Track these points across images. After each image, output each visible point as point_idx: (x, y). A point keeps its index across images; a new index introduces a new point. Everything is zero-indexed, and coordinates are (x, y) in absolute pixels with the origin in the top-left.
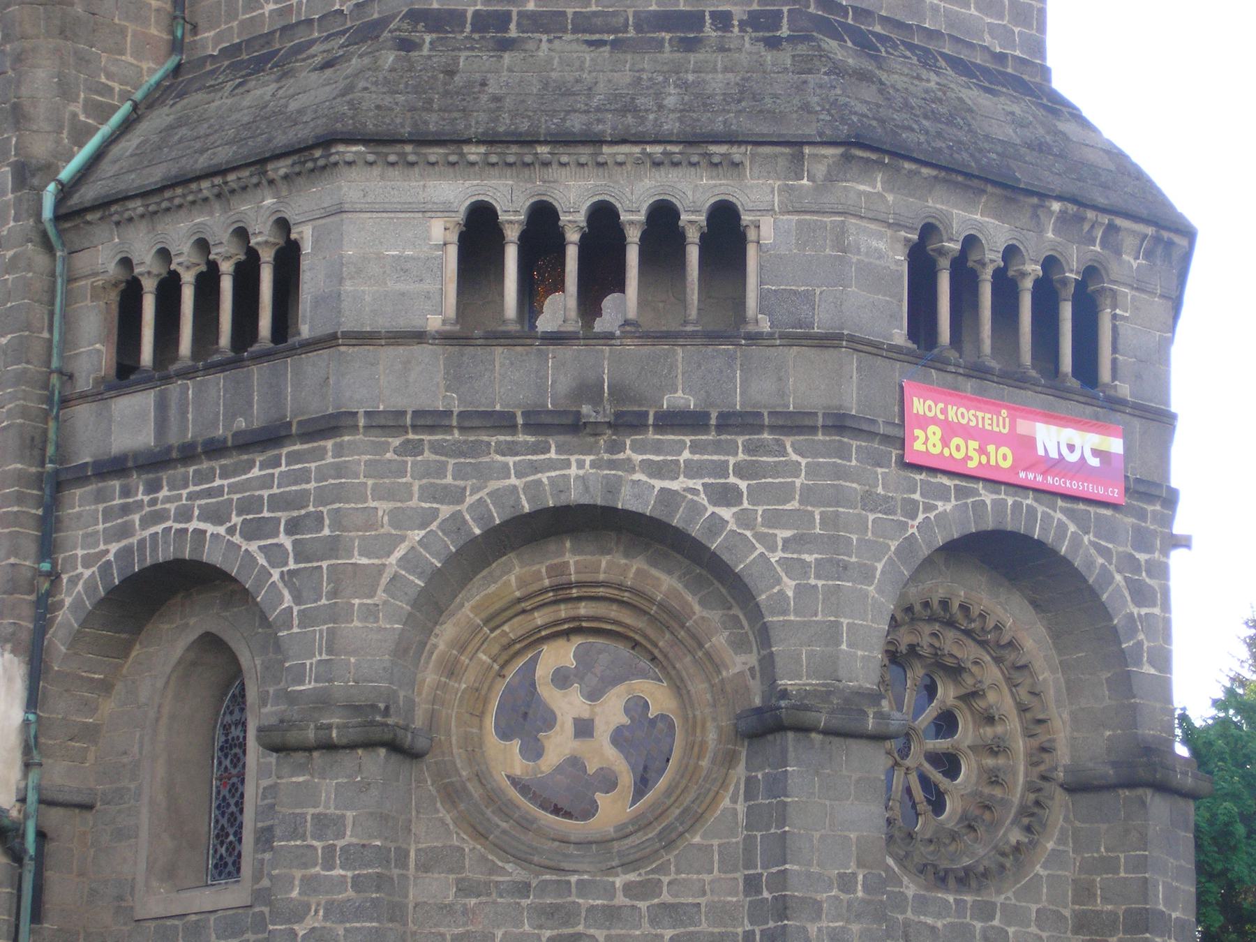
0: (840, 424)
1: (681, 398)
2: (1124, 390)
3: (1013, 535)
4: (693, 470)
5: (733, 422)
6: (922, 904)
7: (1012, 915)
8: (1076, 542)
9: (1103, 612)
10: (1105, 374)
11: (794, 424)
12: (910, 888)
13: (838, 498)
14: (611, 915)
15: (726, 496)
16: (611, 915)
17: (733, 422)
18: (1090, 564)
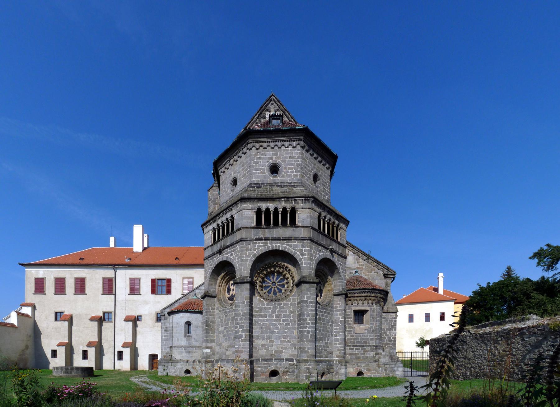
0: (242, 240)
1: (228, 244)
2: (300, 225)
3: (276, 250)
4: (229, 252)
5: (232, 245)
6: (268, 305)
7: (284, 304)
8: (289, 249)
9: (295, 259)
10: (297, 223)
11: (237, 242)
12: (266, 303)
13: (242, 250)
14: (229, 312)
15: (232, 255)
16: (229, 312)
17: (232, 245)
18: (292, 252)
